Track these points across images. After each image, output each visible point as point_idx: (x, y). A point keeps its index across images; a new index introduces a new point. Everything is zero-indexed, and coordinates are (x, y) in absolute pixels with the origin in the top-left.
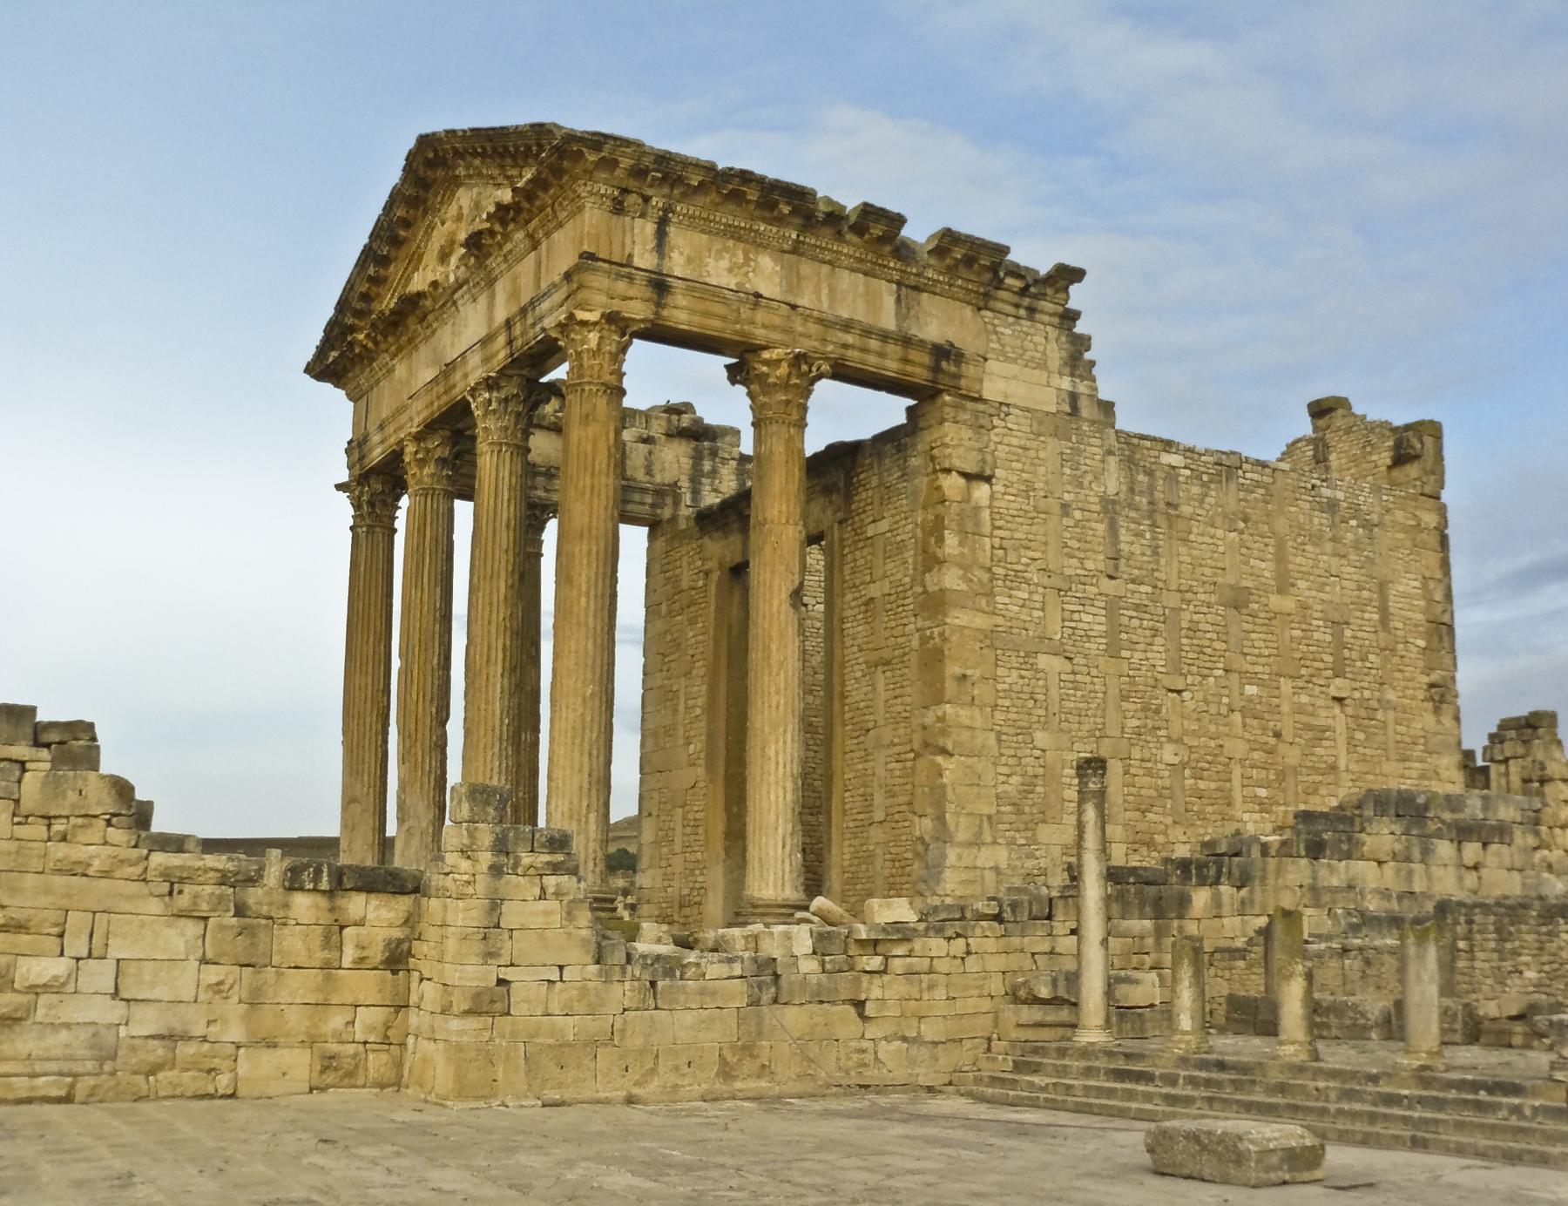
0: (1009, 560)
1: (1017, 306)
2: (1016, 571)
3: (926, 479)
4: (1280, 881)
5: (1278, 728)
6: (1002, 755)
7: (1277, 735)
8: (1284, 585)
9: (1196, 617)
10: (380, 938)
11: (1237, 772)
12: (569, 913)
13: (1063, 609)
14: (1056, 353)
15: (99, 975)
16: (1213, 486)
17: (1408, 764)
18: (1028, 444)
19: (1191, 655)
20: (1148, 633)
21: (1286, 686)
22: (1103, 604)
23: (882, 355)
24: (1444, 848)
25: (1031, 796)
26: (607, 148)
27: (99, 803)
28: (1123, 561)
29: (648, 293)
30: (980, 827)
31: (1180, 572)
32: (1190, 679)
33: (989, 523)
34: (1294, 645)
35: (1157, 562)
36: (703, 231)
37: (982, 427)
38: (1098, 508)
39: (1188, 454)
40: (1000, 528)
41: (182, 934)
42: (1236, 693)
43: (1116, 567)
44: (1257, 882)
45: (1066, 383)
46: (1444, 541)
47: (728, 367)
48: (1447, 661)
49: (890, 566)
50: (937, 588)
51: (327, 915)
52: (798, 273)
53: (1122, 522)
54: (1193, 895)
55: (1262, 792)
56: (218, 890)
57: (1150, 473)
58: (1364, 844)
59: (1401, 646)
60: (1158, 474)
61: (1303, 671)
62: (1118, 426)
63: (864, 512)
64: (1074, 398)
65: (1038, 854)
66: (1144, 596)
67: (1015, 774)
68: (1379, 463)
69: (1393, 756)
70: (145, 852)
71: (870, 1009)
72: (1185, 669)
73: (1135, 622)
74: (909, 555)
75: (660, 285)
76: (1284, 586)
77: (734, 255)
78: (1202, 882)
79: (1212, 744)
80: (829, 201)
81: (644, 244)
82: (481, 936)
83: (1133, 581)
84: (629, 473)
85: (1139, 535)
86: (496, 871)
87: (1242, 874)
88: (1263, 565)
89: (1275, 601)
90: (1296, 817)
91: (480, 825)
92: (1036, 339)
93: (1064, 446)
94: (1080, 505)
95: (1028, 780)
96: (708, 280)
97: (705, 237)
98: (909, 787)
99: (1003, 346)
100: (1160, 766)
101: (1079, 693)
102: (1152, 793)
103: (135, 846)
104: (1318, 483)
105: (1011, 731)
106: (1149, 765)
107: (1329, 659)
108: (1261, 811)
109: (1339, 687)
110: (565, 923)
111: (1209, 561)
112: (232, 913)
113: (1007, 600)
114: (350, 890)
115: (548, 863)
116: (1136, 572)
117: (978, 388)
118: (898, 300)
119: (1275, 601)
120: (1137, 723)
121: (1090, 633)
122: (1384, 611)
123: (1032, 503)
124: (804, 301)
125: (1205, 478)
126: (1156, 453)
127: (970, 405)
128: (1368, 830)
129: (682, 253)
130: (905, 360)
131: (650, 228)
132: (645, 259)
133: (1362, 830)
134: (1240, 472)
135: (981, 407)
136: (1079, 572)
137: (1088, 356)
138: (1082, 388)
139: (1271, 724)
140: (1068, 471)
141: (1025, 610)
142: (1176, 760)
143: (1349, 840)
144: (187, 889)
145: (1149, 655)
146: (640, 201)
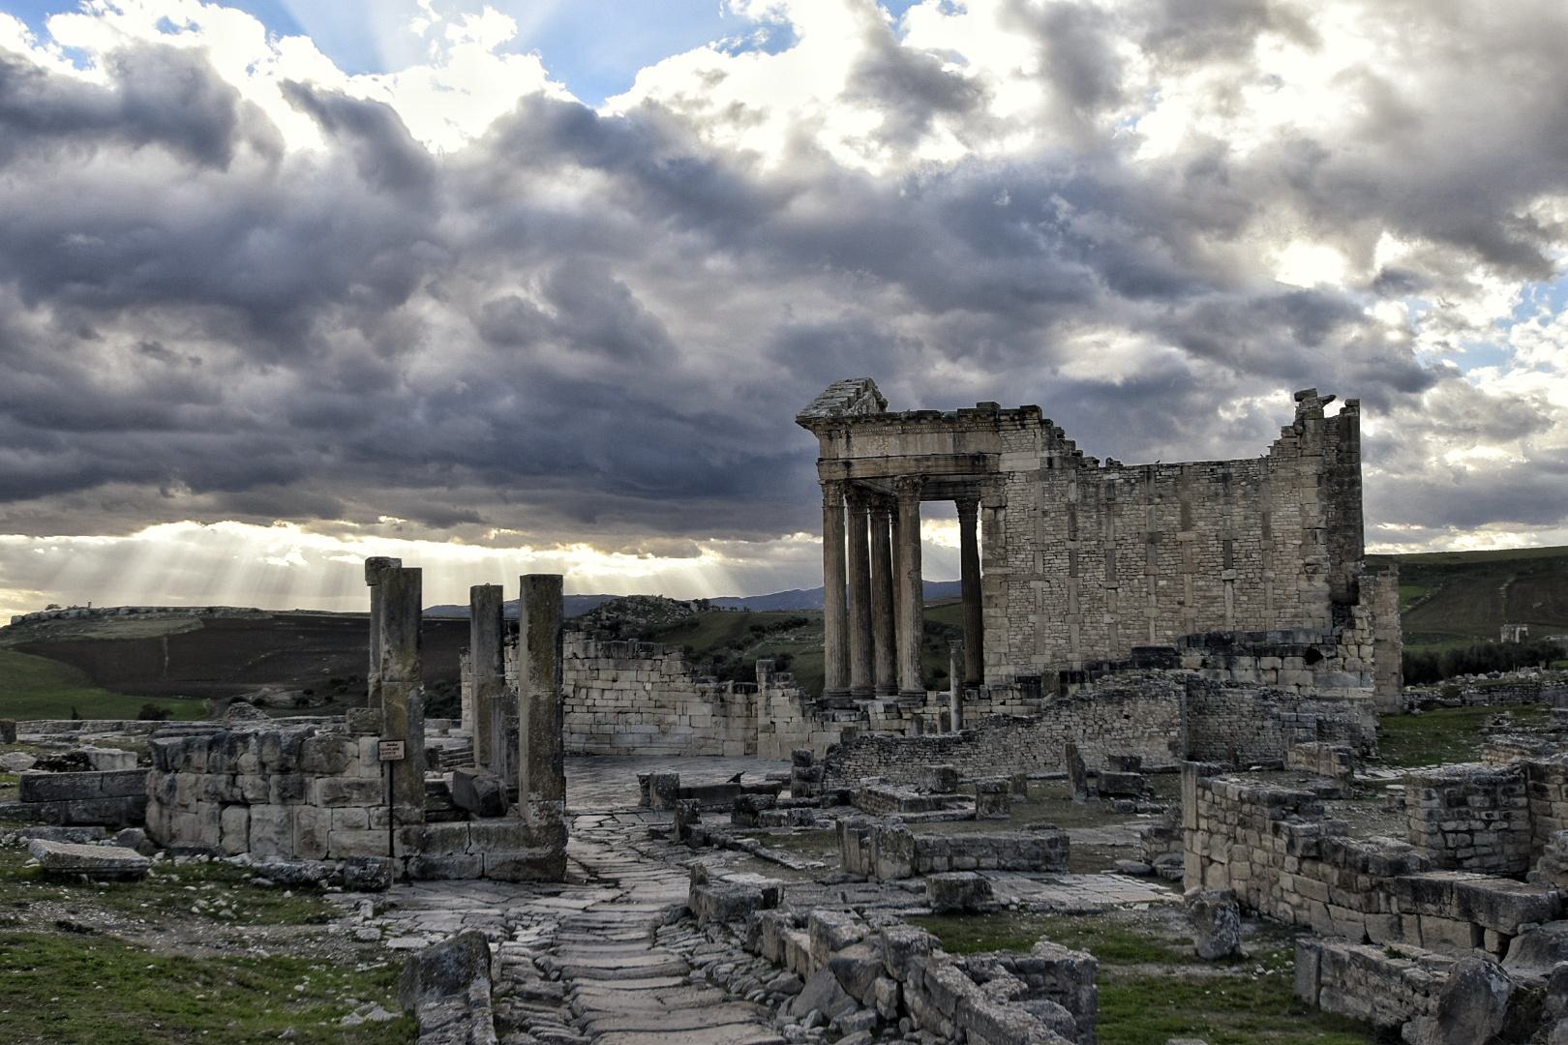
8: (1187, 525)
11: (1153, 623)
15: (685, 720)
23: (946, 466)
24: (1246, 661)
29: (843, 468)
42: (1152, 585)
43: (1075, 536)
57: (1097, 486)
61: (1201, 569)
64: (1050, 460)
72: (1118, 577)
73: (1087, 560)
78: (1073, 682)
86: (767, 688)
89: (1181, 536)
93: (1045, 484)
109: (1227, 574)
118: (954, 439)
119: (1181, 536)
124: (910, 452)
125: (1133, 481)
130: (957, 465)
131: (844, 440)
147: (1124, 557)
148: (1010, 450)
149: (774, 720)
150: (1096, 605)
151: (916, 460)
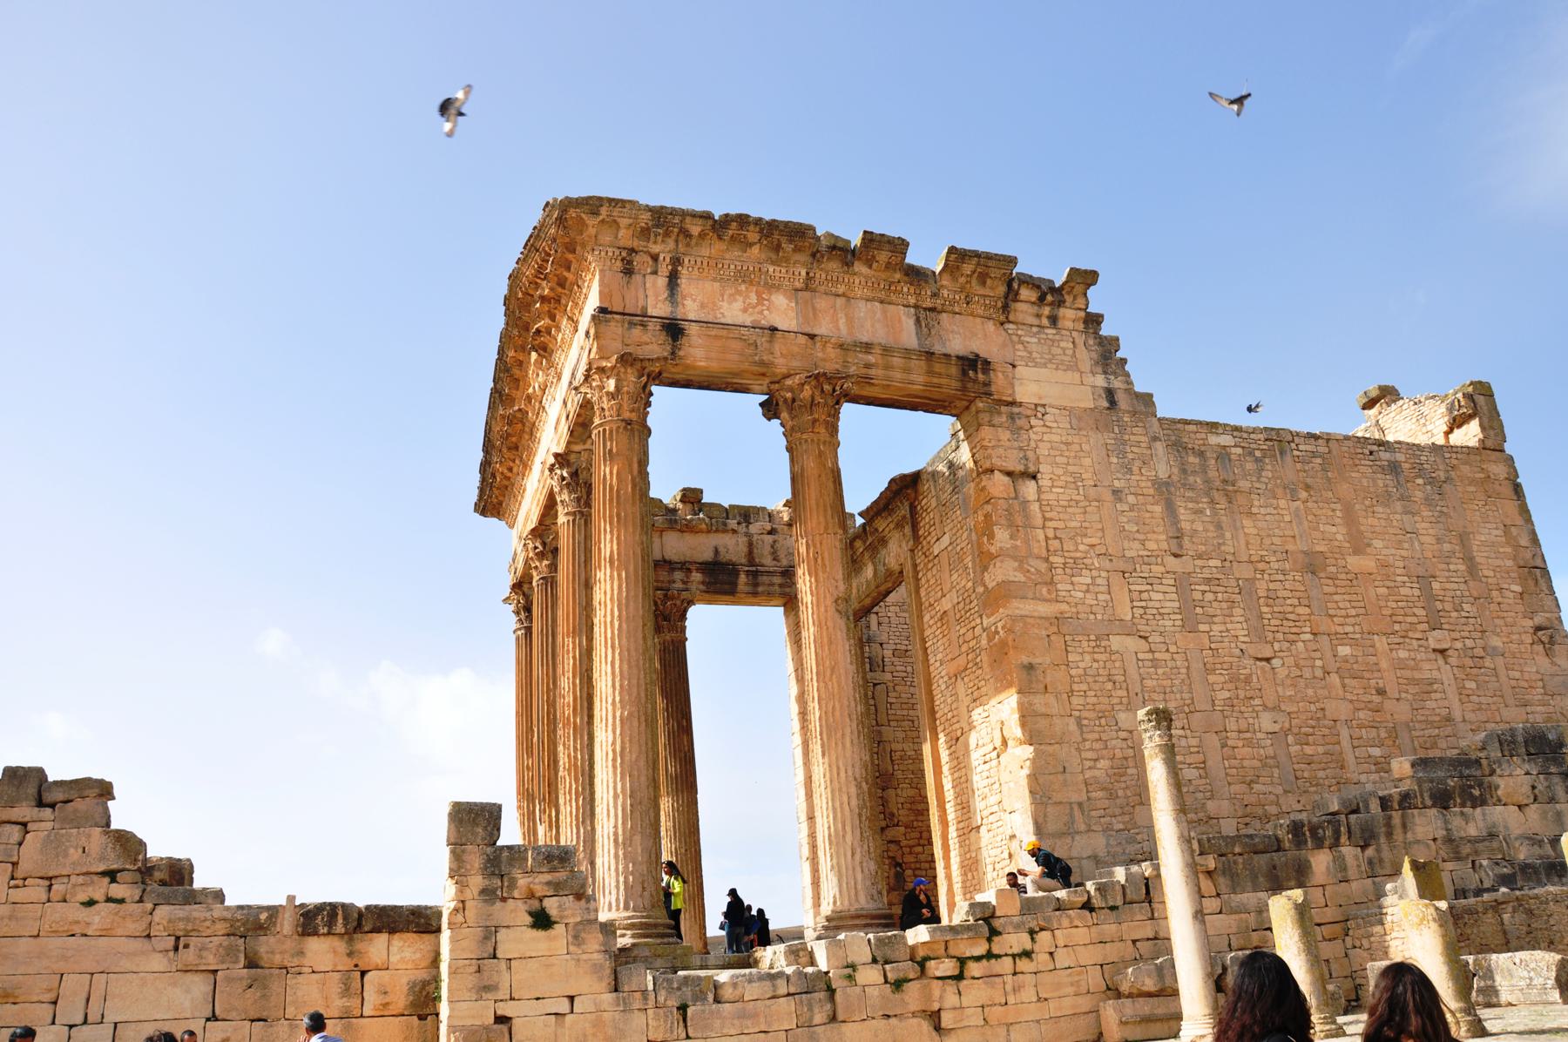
0: (1065, 548)
1: (1038, 316)
2: (1075, 559)
3: (972, 485)
4: (1409, 835)
5: (1381, 685)
6: (1084, 740)
7: (1381, 692)
9: (1272, 586)
10: (405, 980)
11: (1345, 733)
12: (576, 937)
13: (1130, 591)
14: (1086, 357)
16: (1267, 460)
17: (1529, 709)
18: (1070, 439)
19: (1273, 622)
20: (1224, 605)
21: (1381, 643)
22: (1172, 582)
23: (907, 370)
25: (1123, 779)
26: (604, 211)
27: (102, 859)
28: (1186, 539)
29: (663, 337)
30: (1071, 815)
31: (1247, 544)
32: (1277, 646)
33: (1040, 515)
34: (1382, 603)
35: (1222, 536)
36: (714, 280)
37: (1021, 428)
38: (1151, 491)
39: (1235, 433)
40: (1051, 520)
41: (188, 991)
42: (1329, 654)
43: (1181, 547)
44: (1383, 840)
45: (1100, 381)
46: (1518, 490)
47: (762, 405)
48: (1548, 602)
49: (955, 576)
50: (994, 583)
51: (346, 959)
52: (814, 309)
53: (1179, 503)
54: (1312, 860)
55: (1376, 752)
56: (226, 941)
57: (1201, 454)
58: (1497, 787)
59: (1495, 593)
60: (1208, 454)
62: (1159, 415)
63: (930, 533)
64: (1110, 394)
65: (1139, 837)
66: (1214, 570)
67: (1103, 758)
68: (1435, 432)
69: (1511, 701)
70: (149, 906)
71: (947, 1020)
72: (1270, 636)
73: (1209, 596)
74: (968, 561)
75: (674, 330)
76: (1359, 548)
77: (747, 297)
78: (1319, 845)
79: (1313, 708)
80: (829, 235)
81: (657, 296)
82: (475, 968)
83: (1200, 557)
84: (757, 560)
85: (1201, 512)
86: (488, 894)
87: (1363, 831)
88: (1334, 529)
89: (1354, 562)
90: (1413, 766)
91: (469, 847)
92: (1063, 344)
93: (1109, 438)
94: (1132, 490)
95: (1117, 762)
96: (723, 321)
97: (717, 285)
98: (997, 786)
99: (1030, 353)
100: (1259, 735)
101: (1160, 671)
102: (1257, 763)
103: (141, 901)
104: (1375, 448)
105: (1092, 715)
106: (1248, 735)
107: (1423, 613)
108: (1377, 772)
109: (1436, 639)
110: (572, 948)
111: (1276, 531)
112: (242, 963)
113: (1069, 587)
114: (371, 932)
115: (548, 883)
116: (1203, 548)
117: (1010, 392)
118: (918, 321)
119: (1354, 562)
120: (1227, 695)
121: (1161, 611)
122: (1470, 560)
123: (1081, 492)
124: (822, 329)
126: (1204, 436)
127: (1003, 409)
128: (1498, 771)
129: (694, 301)
131: (662, 281)
132: (659, 307)
133: (1492, 773)
134: (1293, 445)
135: (1016, 410)
136: (1141, 553)
137: (1119, 355)
138: (1117, 383)
139: (1373, 682)
140: (1115, 460)
141: (1088, 596)
142: (1276, 728)
143: (1480, 785)
144: (193, 941)
145: (1229, 626)
146: (649, 259)
147: (1271, 598)
148: (1031, 361)
149: (506, 1009)
150: (1242, 694)
151: (841, 346)
